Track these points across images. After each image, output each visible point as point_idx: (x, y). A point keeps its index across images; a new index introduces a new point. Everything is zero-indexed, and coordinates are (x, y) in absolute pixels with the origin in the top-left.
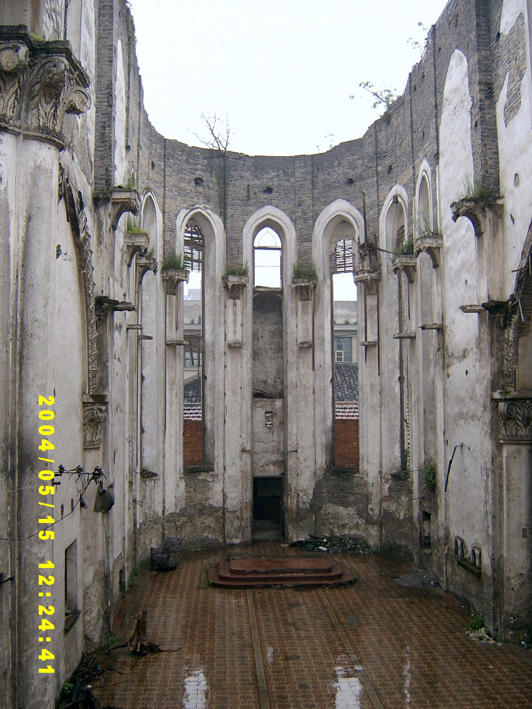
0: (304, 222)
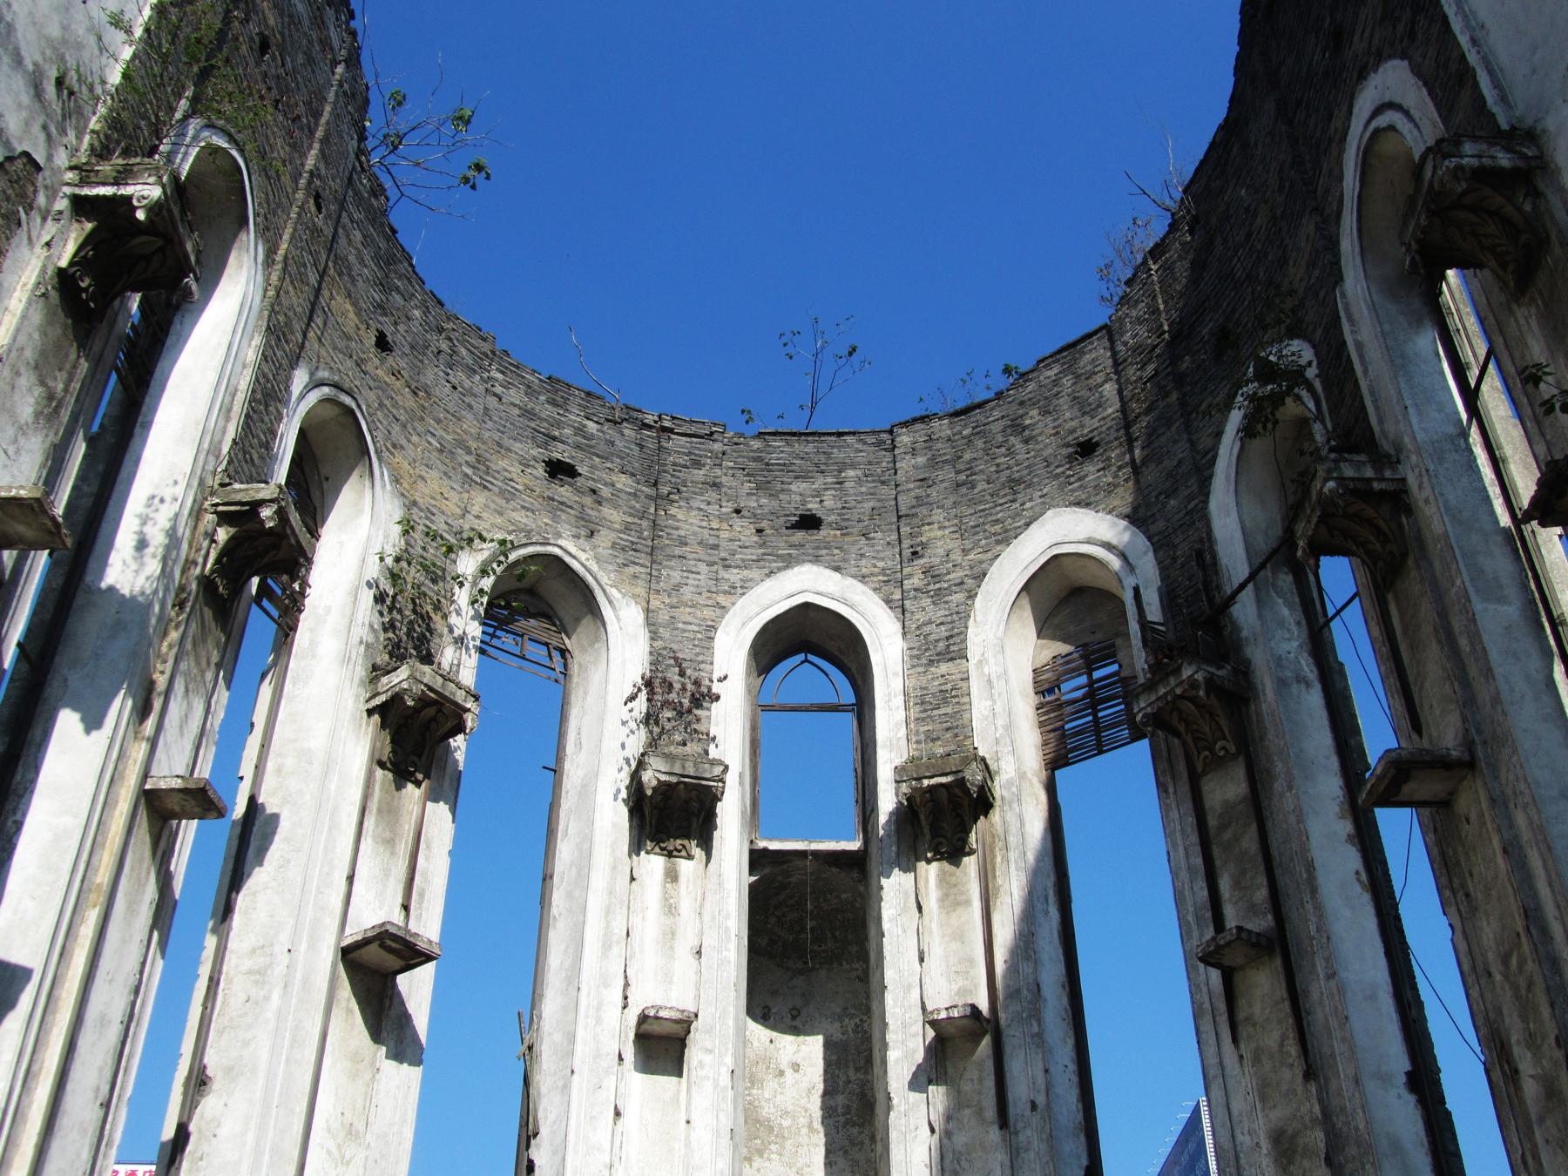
0: (934, 603)
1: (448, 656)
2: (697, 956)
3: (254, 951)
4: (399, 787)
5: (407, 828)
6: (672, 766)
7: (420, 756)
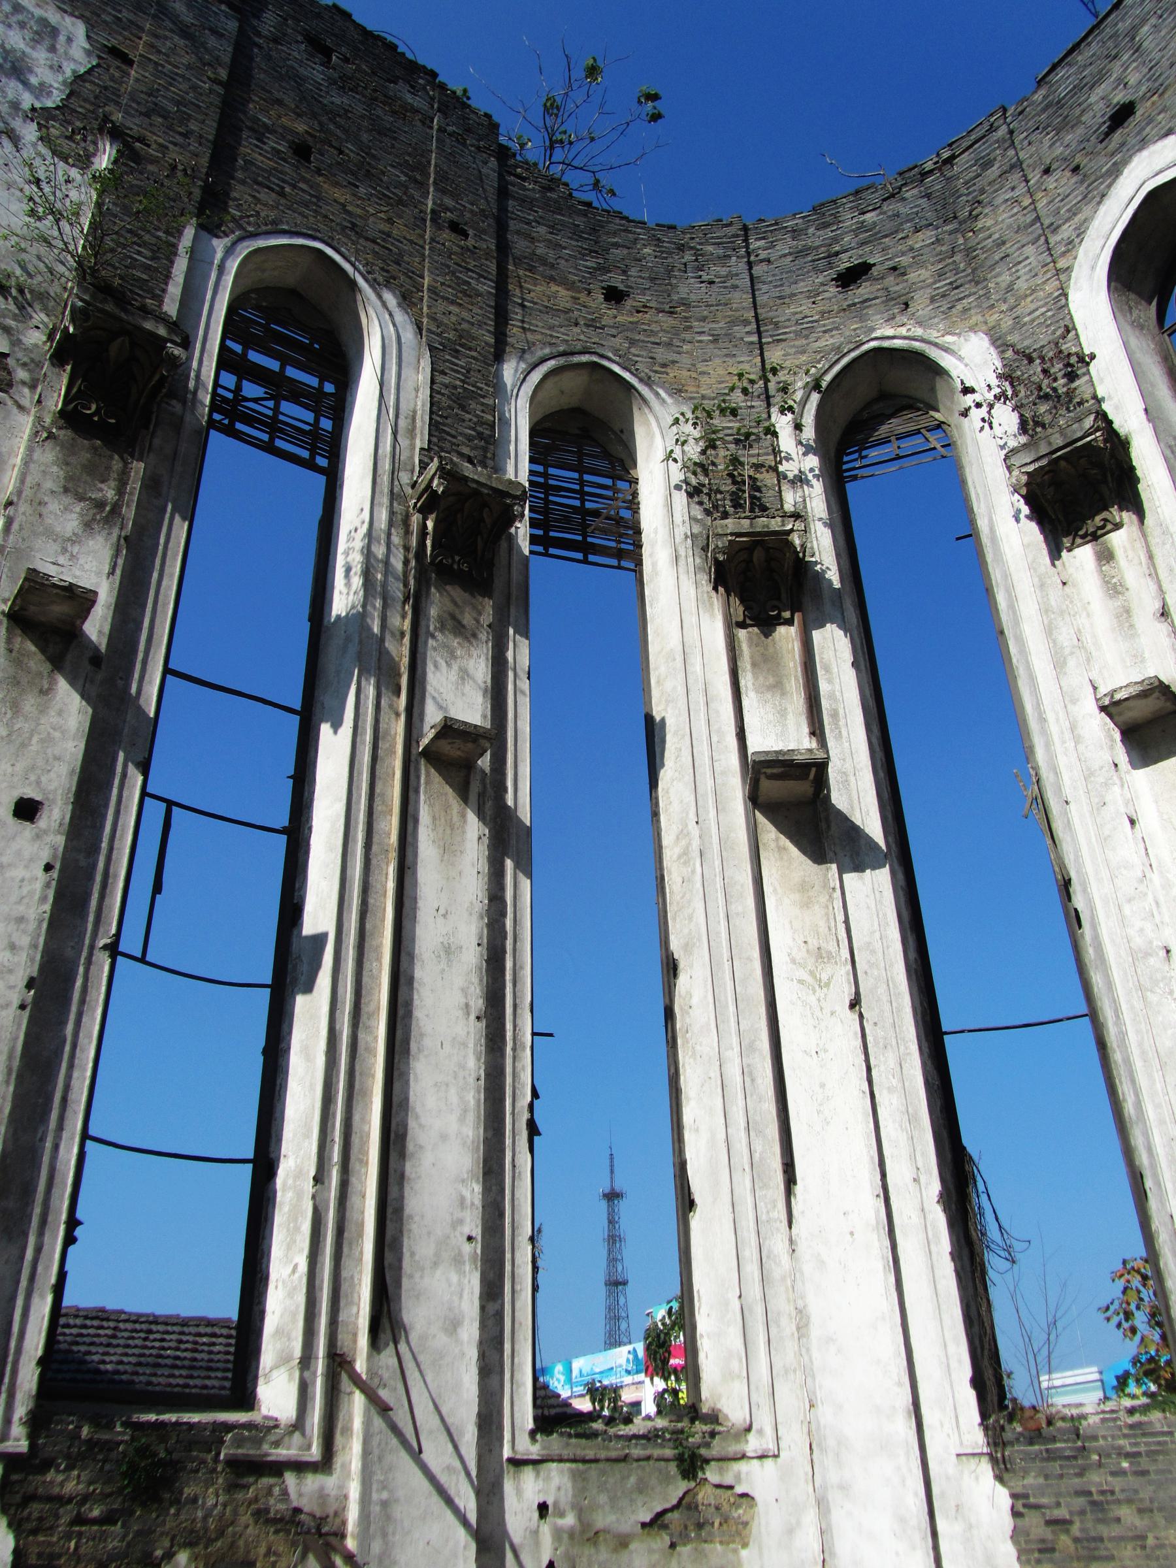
1: (790, 499)
2: (1163, 619)
3: (678, 838)
5: (791, 664)
6: (1037, 450)
7: (779, 599)
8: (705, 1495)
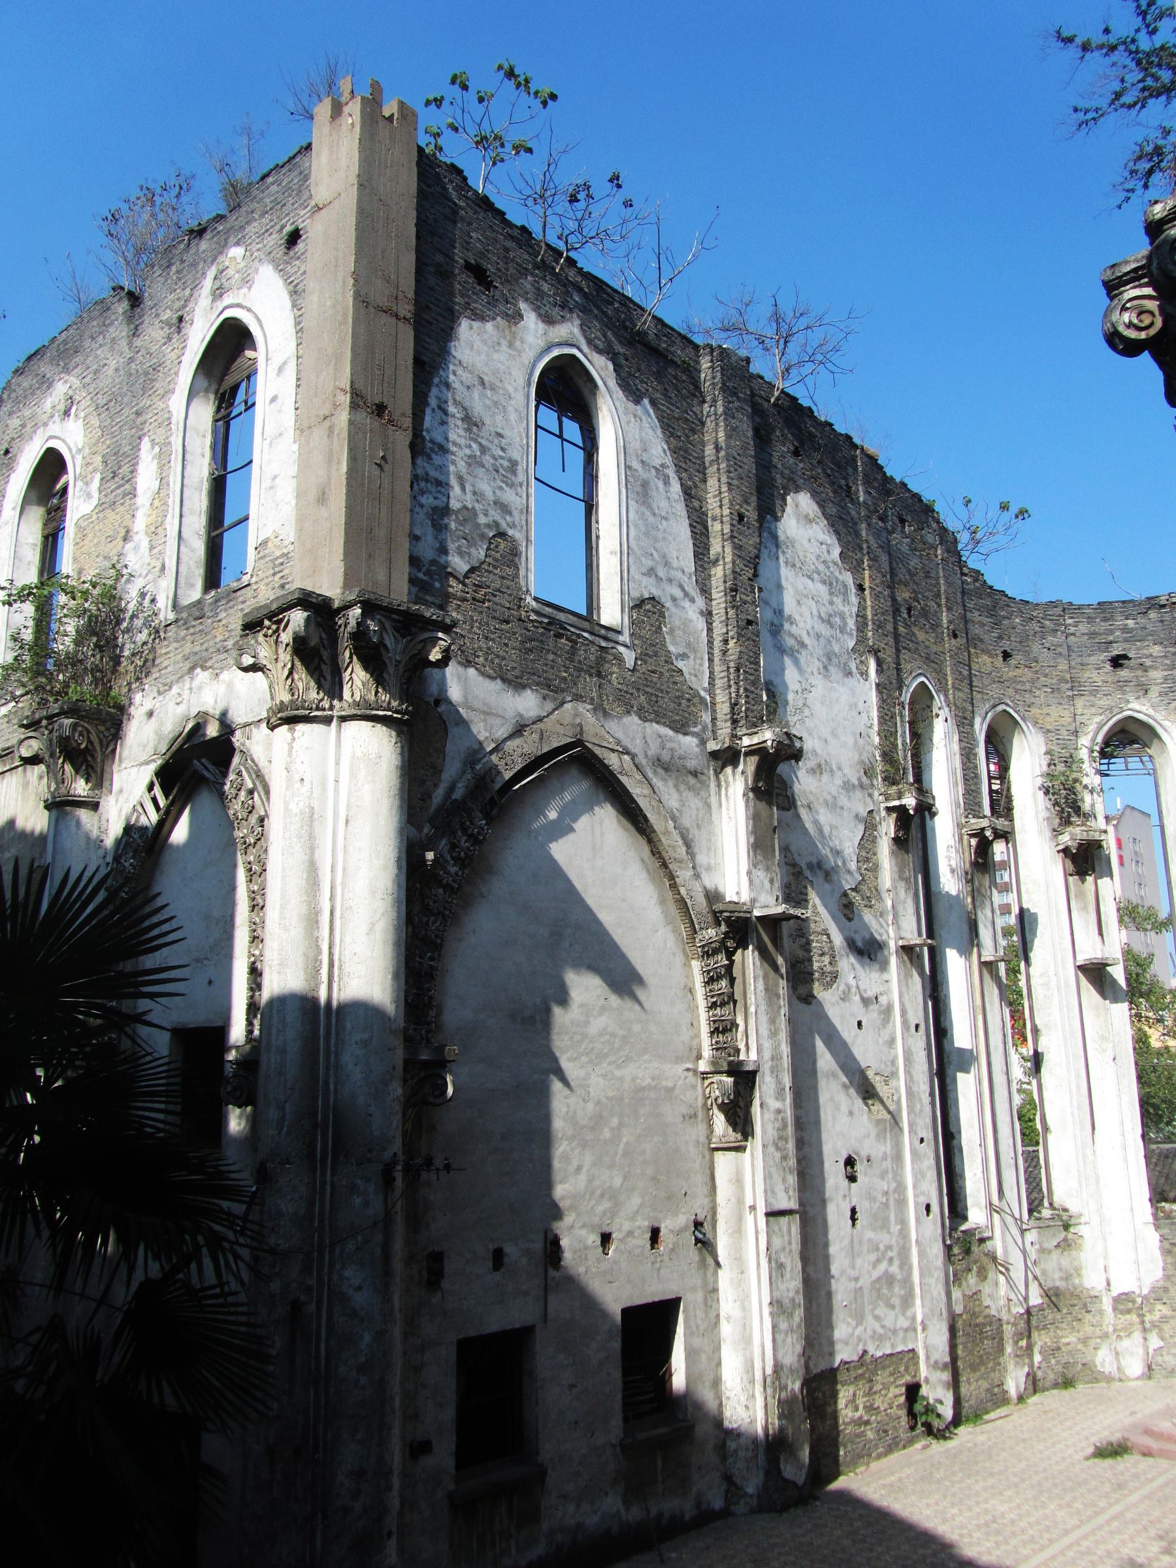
4: (1083, 881)
8: (1070, 1236)
